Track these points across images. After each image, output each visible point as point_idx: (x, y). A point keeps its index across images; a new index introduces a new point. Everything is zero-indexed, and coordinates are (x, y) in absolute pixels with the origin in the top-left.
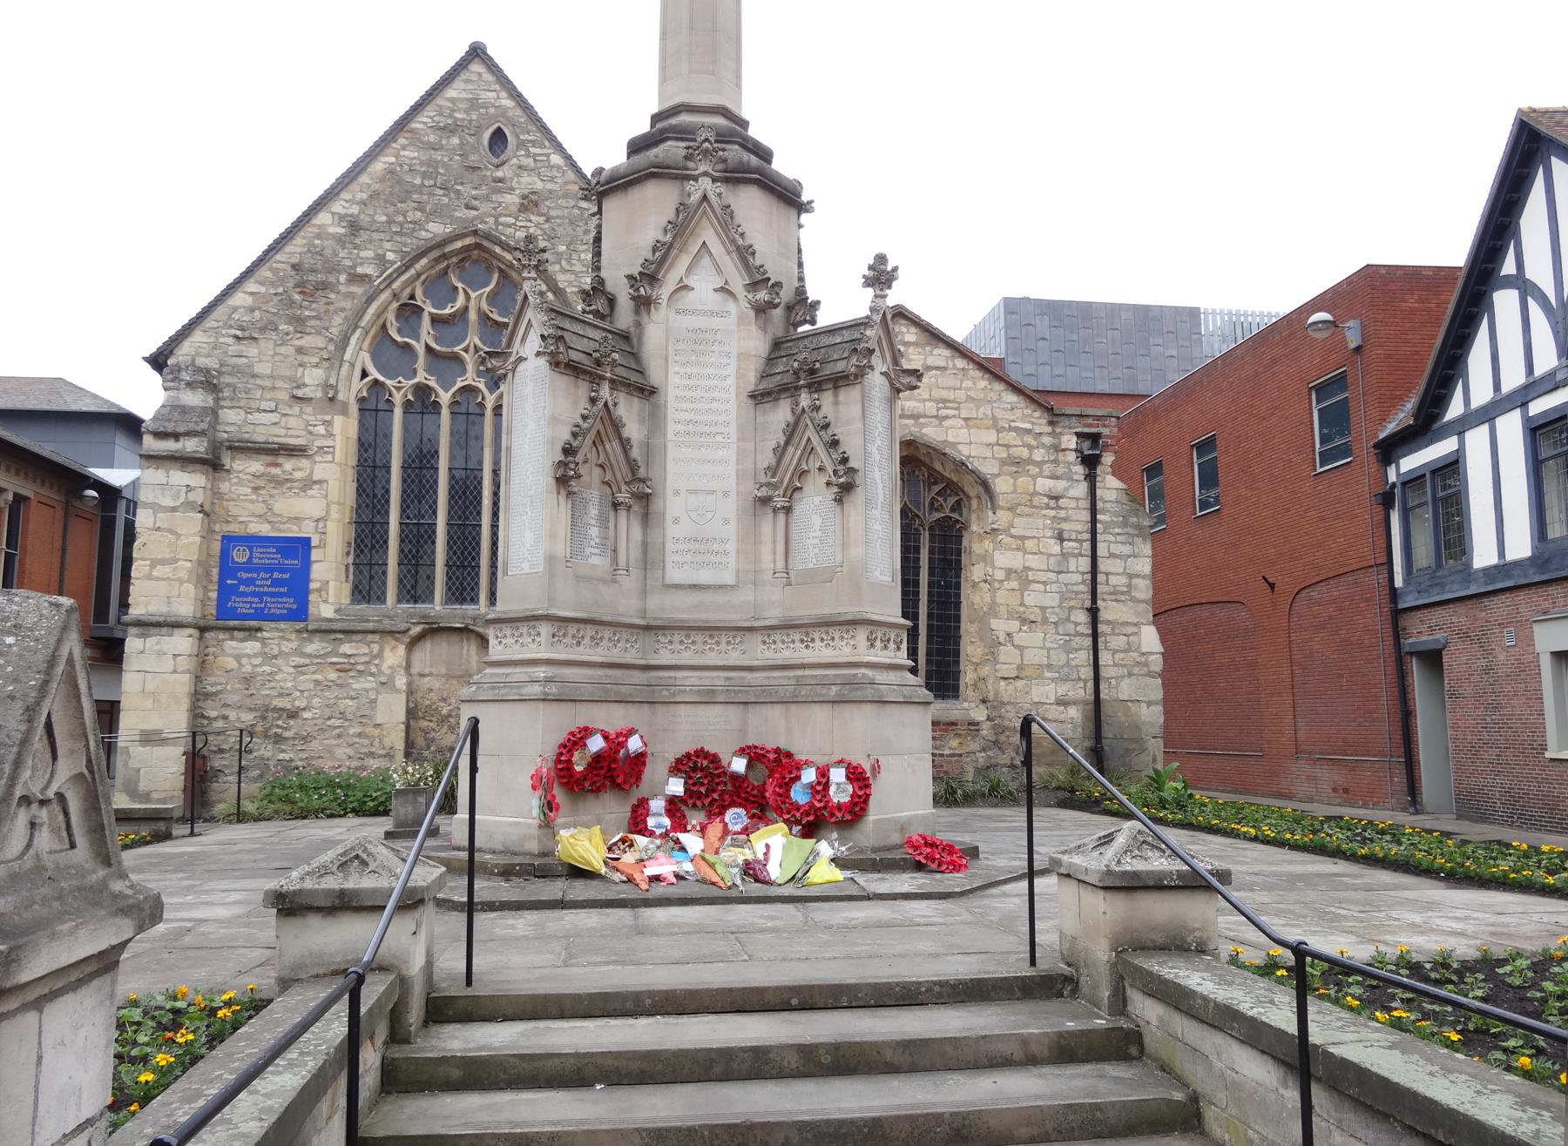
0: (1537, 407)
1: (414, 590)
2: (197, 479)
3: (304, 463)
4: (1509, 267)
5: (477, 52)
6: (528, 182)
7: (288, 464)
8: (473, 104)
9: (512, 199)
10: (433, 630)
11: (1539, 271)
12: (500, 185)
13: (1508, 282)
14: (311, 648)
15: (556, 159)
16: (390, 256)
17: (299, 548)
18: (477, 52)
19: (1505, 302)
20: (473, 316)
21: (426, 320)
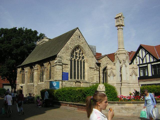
0: (140, 66)
1: (75, 78)
2: (61, 67)
3: (67, 65)
4: (138, 55)
5: (77, 28)
6: (82, 41)
7: (66, 66)
8: (77, 33)
9: (81, 42)
10: (77, 82)
11: (141, 56)
12: (80, 41)
13: (138, 56)
14: (69, 83)
15: (84, 39)
16: (73, 47)
17: (68, 73)
18: (77, 28)
19: (137, 58)
20: (78, 53)
21: (75, 53)
